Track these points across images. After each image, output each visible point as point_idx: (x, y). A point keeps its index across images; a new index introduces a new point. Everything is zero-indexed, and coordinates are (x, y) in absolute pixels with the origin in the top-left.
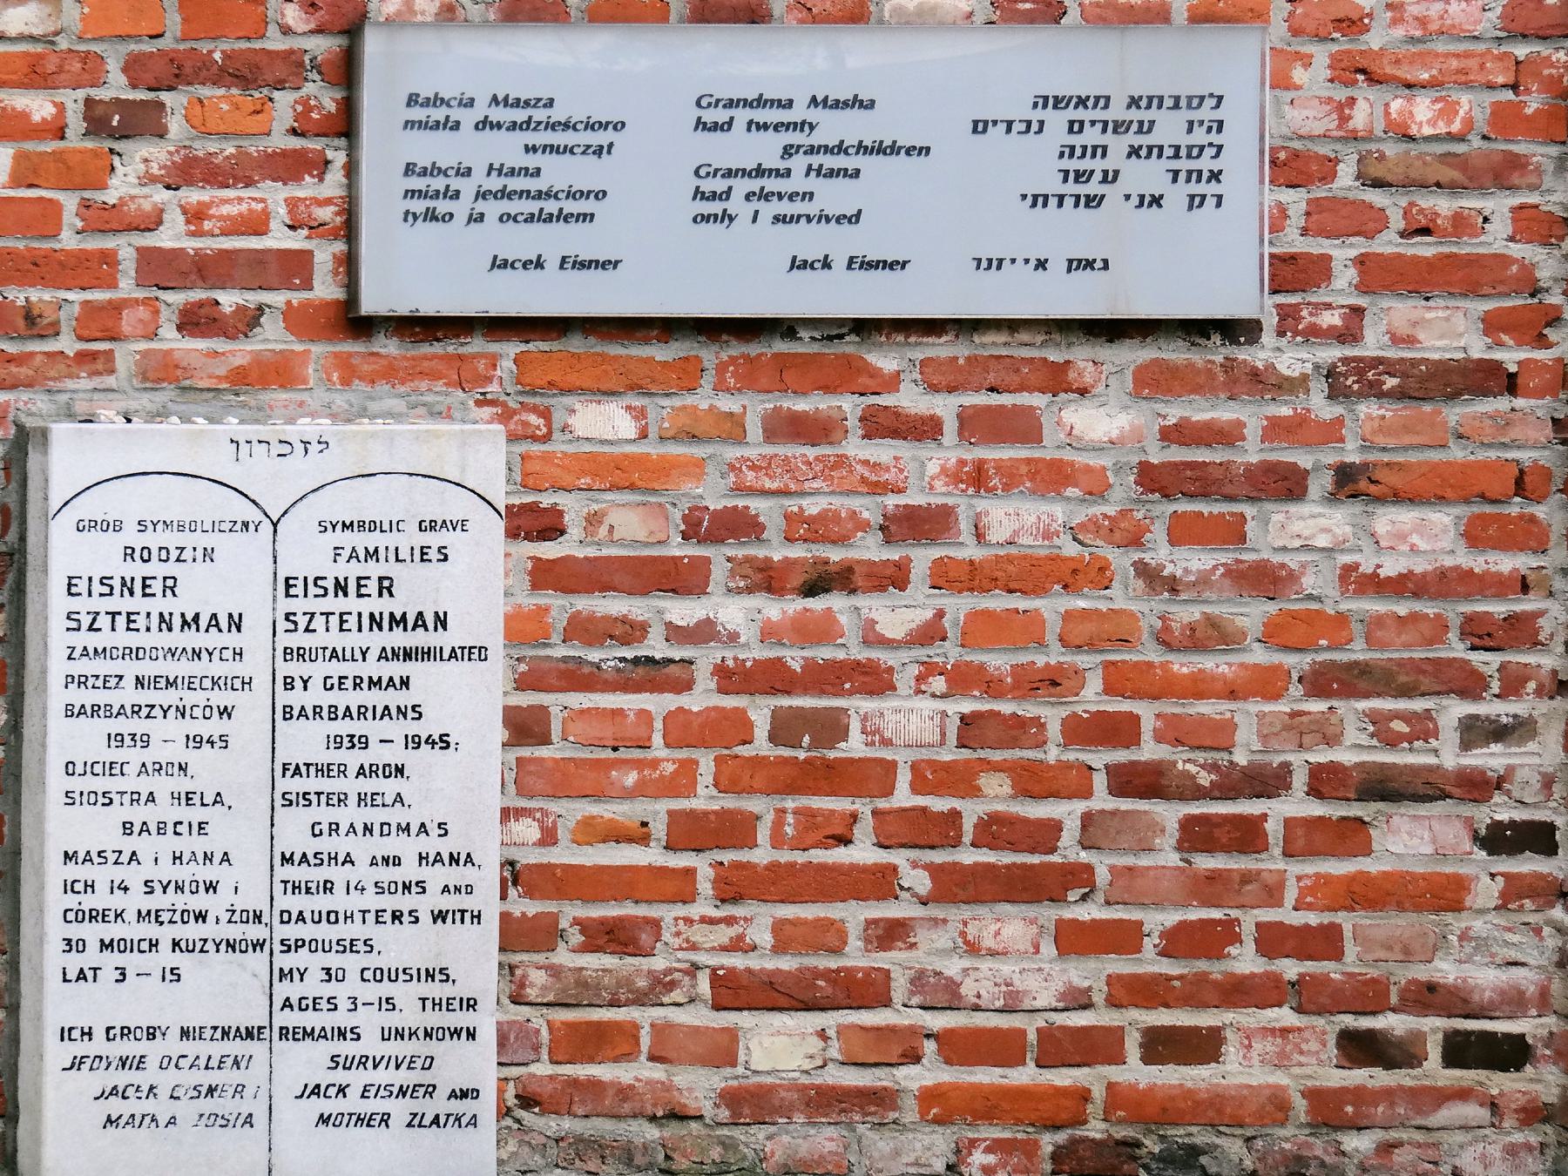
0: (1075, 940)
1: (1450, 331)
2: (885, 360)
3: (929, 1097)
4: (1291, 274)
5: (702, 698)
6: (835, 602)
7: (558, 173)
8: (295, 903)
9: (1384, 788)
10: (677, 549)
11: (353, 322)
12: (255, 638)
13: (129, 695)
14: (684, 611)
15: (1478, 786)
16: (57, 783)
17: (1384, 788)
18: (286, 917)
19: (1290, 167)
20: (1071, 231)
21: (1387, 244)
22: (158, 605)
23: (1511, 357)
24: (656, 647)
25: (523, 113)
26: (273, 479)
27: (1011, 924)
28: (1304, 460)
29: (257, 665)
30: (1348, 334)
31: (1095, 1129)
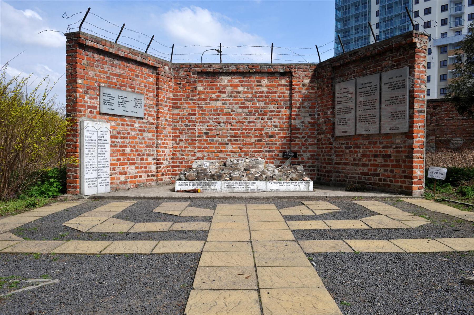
0: (136, 168)
1: (151, 119)
2: (127, 119)
3: (130, 182)
4: (145, 114)
5: (118, 148)
6: (124, 140)
7: (112, 101)
8: (99, 166)
9: (148, 155)
10: (117, 135)
11: (100, 113)
12: (96, 142)
13: (89, 147)
14: (117, 140)
15: (152, 155)
16: (85, 155)
17: (148, 155)
18: (99, 167)
19: (145, 106)
20: (135, 110)
21: (149, 112)
22: (91, 138)
23: (154, 122)
24: (116, 144)
25: (109, 95)
26: (98, 127)
27: (133, 167)
28: (145, 129)
29: (96, 144)
30: (147, 119)
31: (137, 184)
